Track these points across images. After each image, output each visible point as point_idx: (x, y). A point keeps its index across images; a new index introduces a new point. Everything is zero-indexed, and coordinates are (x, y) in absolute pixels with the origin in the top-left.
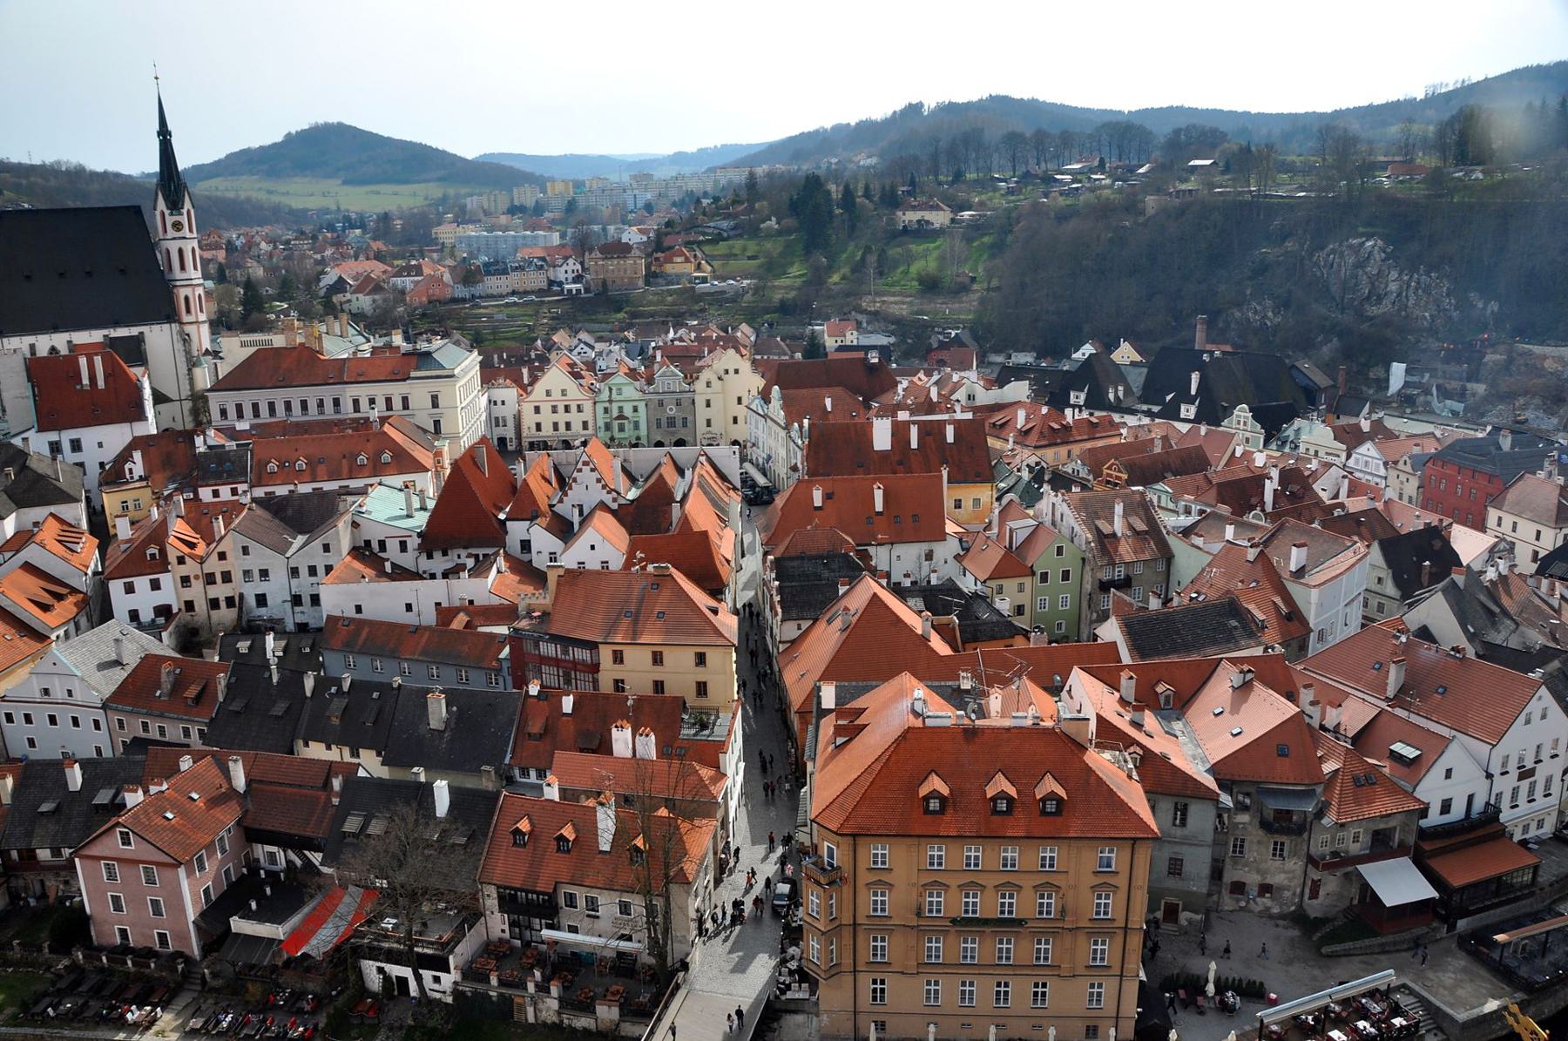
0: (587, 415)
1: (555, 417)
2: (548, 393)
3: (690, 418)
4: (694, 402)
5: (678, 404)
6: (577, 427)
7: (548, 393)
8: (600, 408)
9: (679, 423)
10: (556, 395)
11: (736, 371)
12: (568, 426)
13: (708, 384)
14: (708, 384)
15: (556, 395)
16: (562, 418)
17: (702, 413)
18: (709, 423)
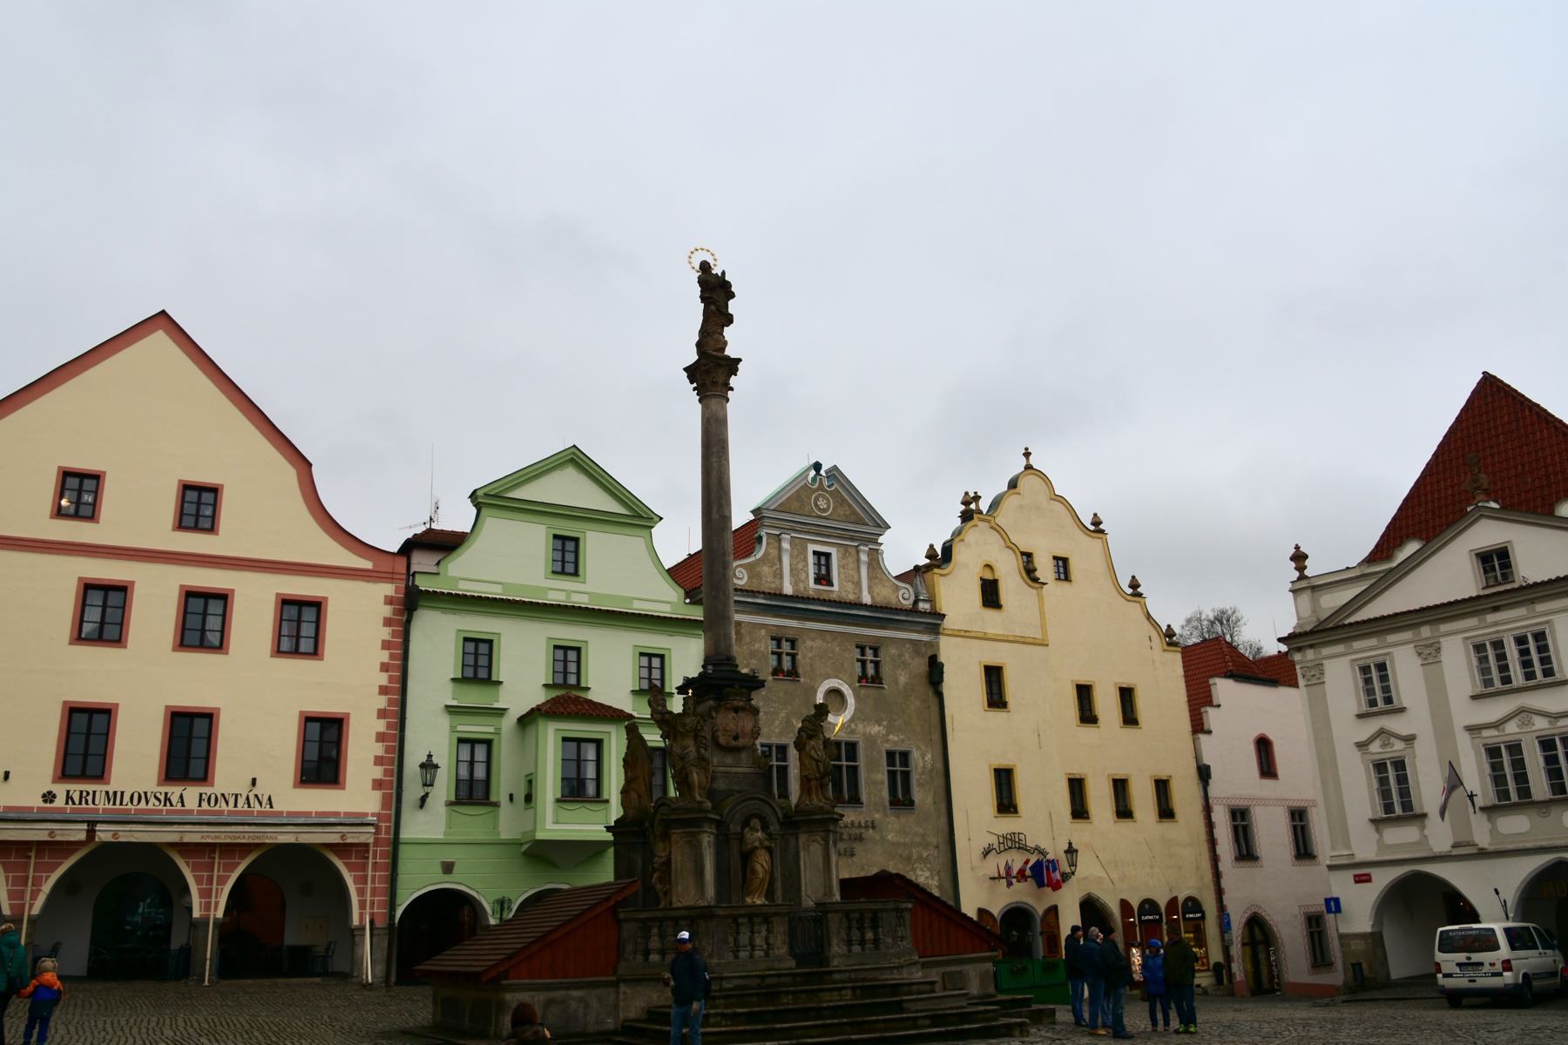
0: (347, 676)
1: (95, 675)
2: (80, 491)
3: (922, 759)
4: (935, 673)
5: (870, 679)
6: (256, 763)
7: (80, 491)
8: (437, 642)
9: (874, 780)
10: (138, 511)
11: (1063, 567)
12: (189, 740)
13: (990, 594)
14: (990, 594)
15: (138, 511)
16: (144, 681)
17: (975, 740)
18: (1006, 804)
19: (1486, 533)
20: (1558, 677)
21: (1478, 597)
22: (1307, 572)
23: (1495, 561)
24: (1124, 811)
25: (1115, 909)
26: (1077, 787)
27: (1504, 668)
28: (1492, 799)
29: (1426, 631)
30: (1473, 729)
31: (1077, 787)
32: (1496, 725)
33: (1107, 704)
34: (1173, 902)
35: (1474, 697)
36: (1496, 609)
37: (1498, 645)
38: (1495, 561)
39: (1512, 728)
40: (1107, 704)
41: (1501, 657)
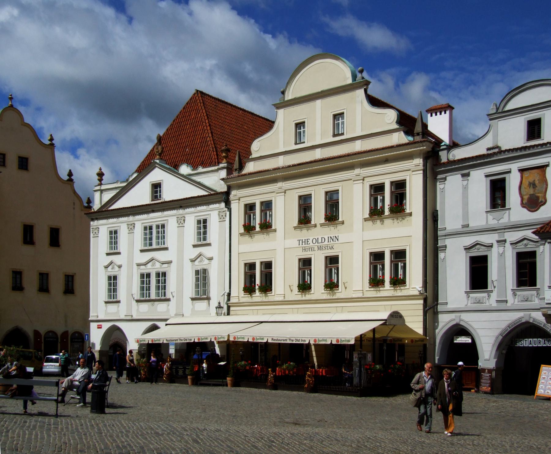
19: (157, 175)
20: (166, 246)
21: (151, 204)
22: (103, 182)
23: (156, 187)
24: (44, 288)
25: (31, 335)
26: (17, 275)
27: (151, 239)
28: (138, 297)
29: (131, 218)
30: (138, 265)
31: (17, 275)
32: (145, 264)
33: (42, 236)
34: (65, 334)
35: (142, 251)
36: (153, 211)
37: (151, 228)
38: (156, 187)
39: (149, 266)
40: (42, 236)
41: (151, 233)
